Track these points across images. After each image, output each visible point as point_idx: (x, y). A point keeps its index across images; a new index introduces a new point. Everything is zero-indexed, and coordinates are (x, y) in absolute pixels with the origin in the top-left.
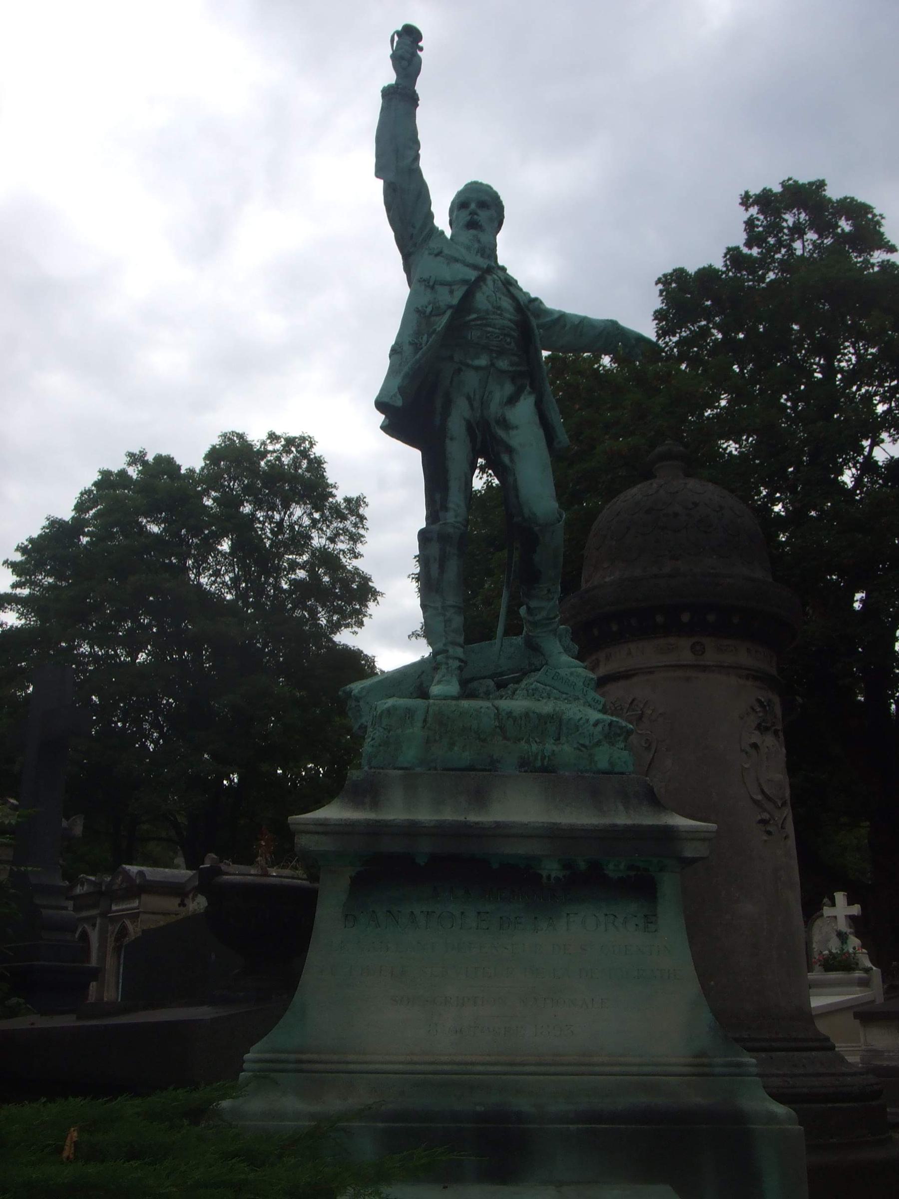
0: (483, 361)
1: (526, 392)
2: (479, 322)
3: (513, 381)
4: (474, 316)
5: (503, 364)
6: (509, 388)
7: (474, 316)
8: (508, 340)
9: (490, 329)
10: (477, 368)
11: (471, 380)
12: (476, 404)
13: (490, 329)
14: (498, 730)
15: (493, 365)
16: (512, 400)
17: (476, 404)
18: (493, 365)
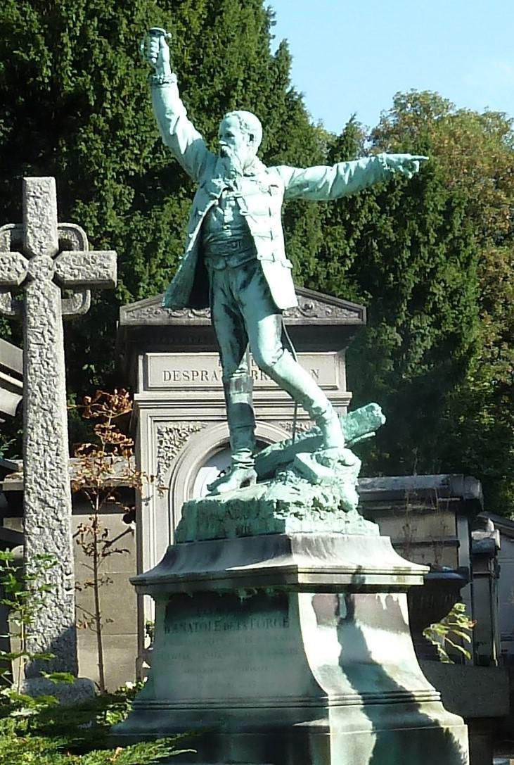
0: (221, 266)
1: (255, 275)
2: (213, 240)
3: (245, 269)
4: (211, 235)
5: (234, 262)
6: (242, 276)
7: (211, 235)
8: (234, 244)
9: (220, 242)
10: (220, 270)
11: (220, 277)
12: (227, 292)
13: (220, 242)
14: (228, 514)
15: (227, 265)
16: (245, 285)
17: (227, 292)
18: (227, 265)
